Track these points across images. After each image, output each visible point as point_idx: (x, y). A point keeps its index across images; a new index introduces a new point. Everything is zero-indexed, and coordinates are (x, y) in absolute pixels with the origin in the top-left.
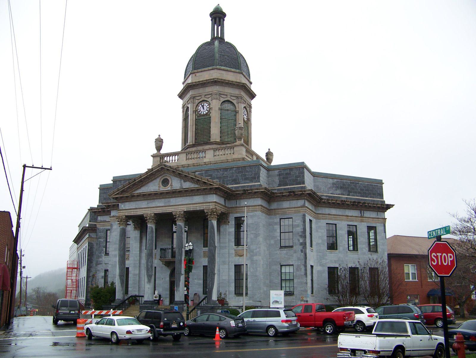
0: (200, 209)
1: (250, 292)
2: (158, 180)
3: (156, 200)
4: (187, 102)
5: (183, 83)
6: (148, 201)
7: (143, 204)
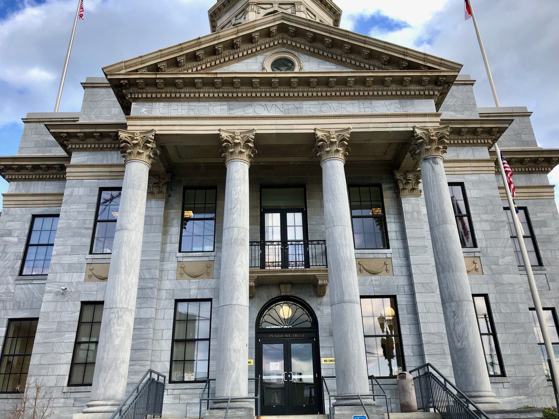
0: (395, 129)
1: (512, 369)
2: (260, 58)
4: (236, 17)
6: (230, 103)
7: (218, 109)
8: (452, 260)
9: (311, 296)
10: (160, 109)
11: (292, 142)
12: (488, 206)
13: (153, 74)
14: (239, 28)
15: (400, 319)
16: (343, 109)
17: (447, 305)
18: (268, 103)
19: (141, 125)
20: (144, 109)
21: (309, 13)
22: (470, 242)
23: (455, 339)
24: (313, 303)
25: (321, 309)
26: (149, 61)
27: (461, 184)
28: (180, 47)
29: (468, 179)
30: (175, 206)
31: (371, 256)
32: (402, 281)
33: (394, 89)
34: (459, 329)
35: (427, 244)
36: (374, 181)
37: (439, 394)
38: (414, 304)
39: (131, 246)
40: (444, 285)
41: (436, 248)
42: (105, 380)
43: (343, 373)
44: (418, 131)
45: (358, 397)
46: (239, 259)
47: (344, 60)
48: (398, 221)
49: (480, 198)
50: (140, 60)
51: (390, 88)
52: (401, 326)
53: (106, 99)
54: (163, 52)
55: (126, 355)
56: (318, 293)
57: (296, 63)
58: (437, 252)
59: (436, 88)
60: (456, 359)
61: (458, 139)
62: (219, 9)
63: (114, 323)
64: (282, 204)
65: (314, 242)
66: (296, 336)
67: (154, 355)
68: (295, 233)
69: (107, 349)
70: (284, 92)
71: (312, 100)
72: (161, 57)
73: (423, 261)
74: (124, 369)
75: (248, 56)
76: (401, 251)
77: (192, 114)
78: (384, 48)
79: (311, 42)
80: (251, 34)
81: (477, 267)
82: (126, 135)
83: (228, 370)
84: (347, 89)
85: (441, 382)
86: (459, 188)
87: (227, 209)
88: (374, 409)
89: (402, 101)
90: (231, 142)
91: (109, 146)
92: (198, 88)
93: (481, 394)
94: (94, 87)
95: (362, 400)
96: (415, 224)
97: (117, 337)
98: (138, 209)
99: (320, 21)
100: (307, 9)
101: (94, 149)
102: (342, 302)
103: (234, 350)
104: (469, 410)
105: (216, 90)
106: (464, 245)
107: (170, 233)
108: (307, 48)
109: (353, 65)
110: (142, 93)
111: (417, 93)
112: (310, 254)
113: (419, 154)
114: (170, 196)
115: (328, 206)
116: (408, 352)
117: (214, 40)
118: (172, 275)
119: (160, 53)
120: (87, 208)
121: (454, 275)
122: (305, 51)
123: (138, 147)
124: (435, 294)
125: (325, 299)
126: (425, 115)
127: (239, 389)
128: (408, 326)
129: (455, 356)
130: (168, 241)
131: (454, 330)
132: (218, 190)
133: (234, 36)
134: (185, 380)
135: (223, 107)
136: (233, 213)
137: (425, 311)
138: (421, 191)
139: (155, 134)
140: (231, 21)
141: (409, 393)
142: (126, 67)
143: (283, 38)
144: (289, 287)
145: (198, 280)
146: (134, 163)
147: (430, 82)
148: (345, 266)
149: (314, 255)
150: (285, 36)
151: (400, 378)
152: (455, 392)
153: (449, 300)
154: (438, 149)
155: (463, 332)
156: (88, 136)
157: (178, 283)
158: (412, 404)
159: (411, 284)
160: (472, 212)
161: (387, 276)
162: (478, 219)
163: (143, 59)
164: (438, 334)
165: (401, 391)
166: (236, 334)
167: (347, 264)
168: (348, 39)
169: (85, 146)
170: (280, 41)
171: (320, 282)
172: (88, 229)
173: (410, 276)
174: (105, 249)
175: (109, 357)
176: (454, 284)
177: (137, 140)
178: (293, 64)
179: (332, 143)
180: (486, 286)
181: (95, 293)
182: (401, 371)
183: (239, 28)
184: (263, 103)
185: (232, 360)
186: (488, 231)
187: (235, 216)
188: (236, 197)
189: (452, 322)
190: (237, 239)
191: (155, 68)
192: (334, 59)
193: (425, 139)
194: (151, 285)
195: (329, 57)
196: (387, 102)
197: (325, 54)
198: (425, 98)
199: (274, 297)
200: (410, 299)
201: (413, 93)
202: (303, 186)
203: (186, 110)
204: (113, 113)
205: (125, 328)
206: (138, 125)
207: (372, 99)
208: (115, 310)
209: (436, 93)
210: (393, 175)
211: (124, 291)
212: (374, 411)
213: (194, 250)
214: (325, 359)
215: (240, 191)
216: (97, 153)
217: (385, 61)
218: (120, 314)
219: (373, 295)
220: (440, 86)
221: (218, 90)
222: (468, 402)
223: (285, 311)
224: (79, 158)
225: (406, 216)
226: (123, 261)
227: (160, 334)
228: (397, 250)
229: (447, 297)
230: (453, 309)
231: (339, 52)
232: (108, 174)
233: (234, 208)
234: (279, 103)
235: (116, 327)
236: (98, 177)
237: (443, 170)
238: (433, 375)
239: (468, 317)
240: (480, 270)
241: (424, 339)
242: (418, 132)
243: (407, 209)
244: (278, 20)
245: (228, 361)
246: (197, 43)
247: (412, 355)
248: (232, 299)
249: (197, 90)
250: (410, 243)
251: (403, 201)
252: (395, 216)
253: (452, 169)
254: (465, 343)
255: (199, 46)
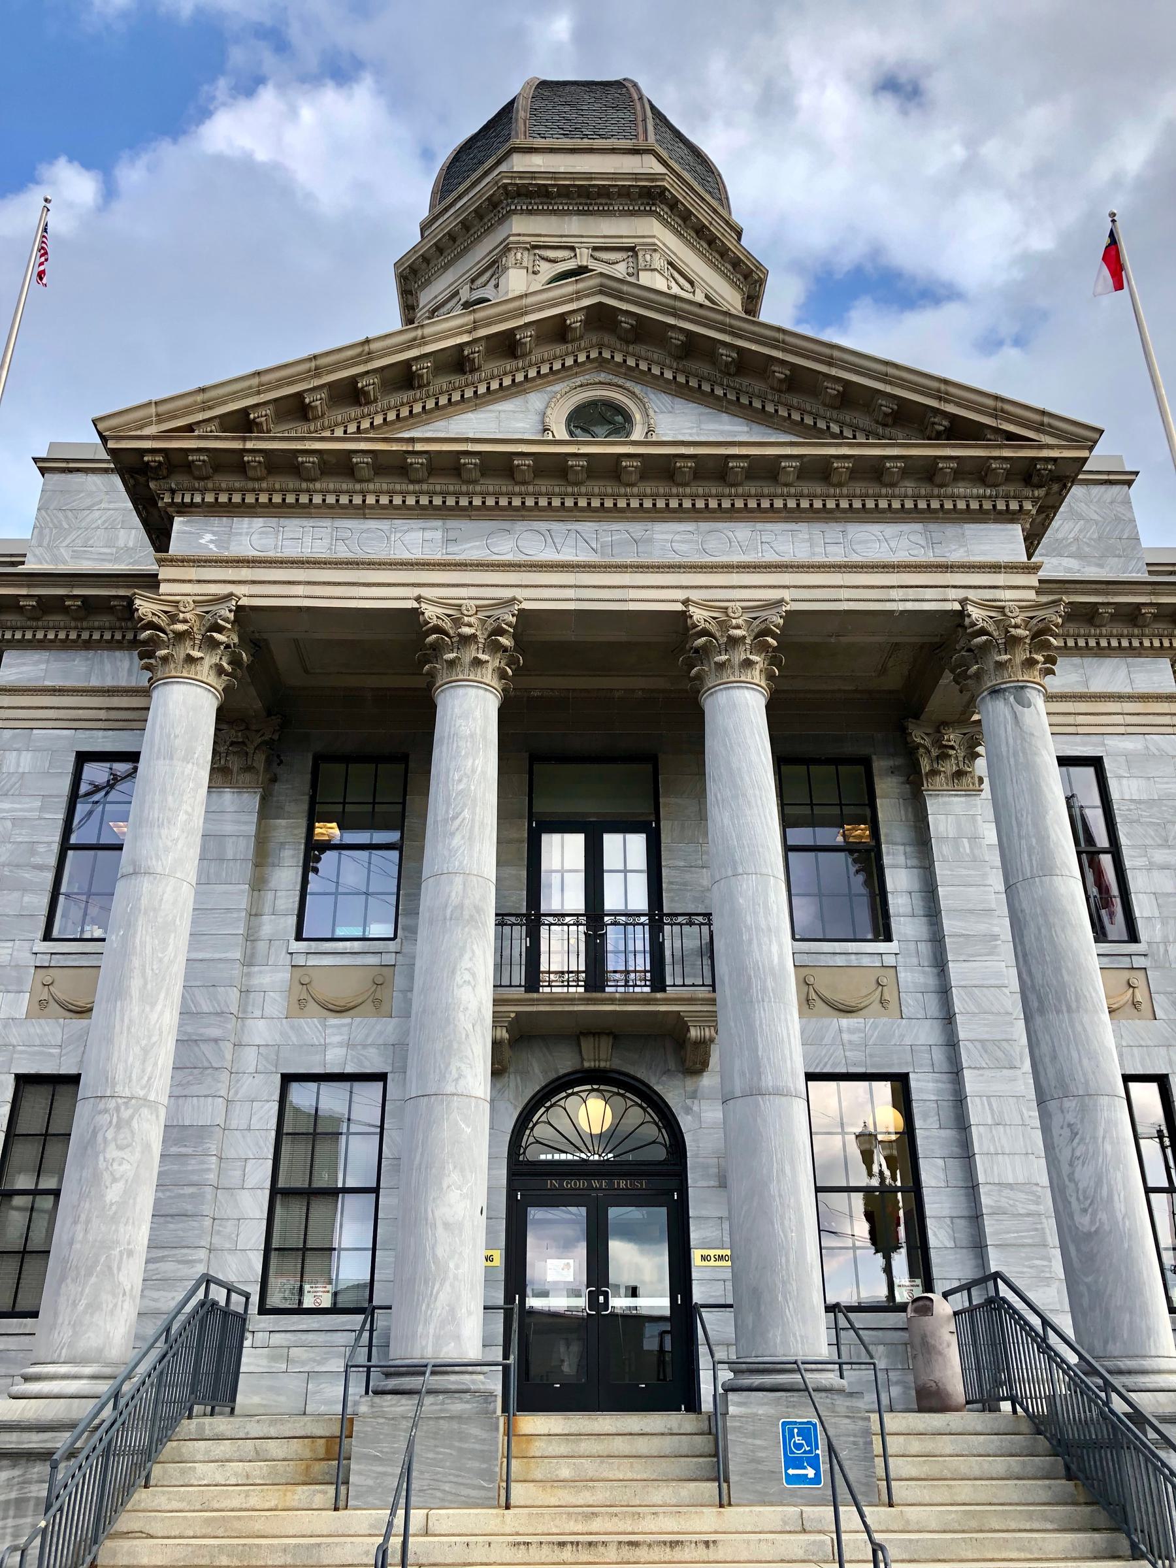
0: (910, 606)
2: (535, 400)
3: (520, 526)
4: (473, 281)
5: (424, 228)
6: (451, 524)
7: (416, 539)
8: (1066, 977)
9: (667, 1072)
10: (252, 536)
11: (622, 636)
12: (1169, 826)
13: (233, 439)
14: (480, 315)
15: (919, 1141)
16: (766, 546)
17: (1052, 1105)
18: (555, 526)
19: (199, 581)
20: (209, 536)
21: (676, 275)
22: (1117, 927)
23: (1075, 1205)
24: (673, 1093)
25: (695, 1108)
26: (225, 403)
27: (1097, 763)
28: (313, 364)
29: (1115, 750)
30: (290, 807)
31: (840, 961)
32: (927, 1033)
33: (910, 492)
34: (1085, 1175)
35: (996, 930)
36: (849, 749)
37: (1026, 1361)
38: (959, 1101)
39: (160, 920)
40: (1045, 1048)
41: (1022, 943)
42: (75, 1304)
43: (751, 1298)
44: (975, 613)
45: (795, 1367)
46: (465, 963)
47: (770, 408)
48: (915, 862)
49: (1151, 803)
50: (199, 398)
51: (897, 491)
52: (921, 1161)
53: (103, 506)
54: (265, 378)
55: (138, 1232)
56: (688, 1064)
57: (638, 416)
58: (1025, 955)
59: (1028, 492)
60: (1075, 1260)
61: (1087, 637)
62: (425, 259)
63: (105, 1139)
64: (590, 807)
65: (680, 919)
66: (622, 1185)
67: (219, 1232)
68: (626, 892)
69: (83, 1217)
70: (602, 496)
71: (680, 520)
72: (259, 393)
73: (987, 976)
74: (132, 1273)
75: (505, 393)
76: (925, 948)
77: (343, 553)
78: (884, 378)
79: (678, 358)
80: (511, 332)
81: (1139, 998)
82: (156, 607)
83: (426, 1282)
84: (779, 491)
85: (1032, 1329)
86: (1090, 771)
87: (436, 822)
88: (842, 1403)
89: (932, 526)
90: (451, 632)
91: (107, 636)
92: (360, 481)
93: (1147, 1364)
94: (70, 471)
95: (808, 1376)
96: (964, 872)
97: (115, 1180)
98: (182, 817)
99: (707, 297)
100: (670, 264)
101: (66, 645)
102: (755, 1092)
103: (447, 1225)
104: (1112, 1411)
105: (411, 487)
106: (1100, 934)
107: (272, 885)
108: (668, 375)
109: (795, 423)
110: (203, 491)
111: (974, 505)
112: (668, 953)
113: (978, 676)
114: (274, 780)
115: (719, 816)
116: (938, 1236)
117: (409, 348)
118: (276, 1003)
119: (255, 381)
120: (42, 809)
121: (1071, 1020)
122: (661, 382)
123: (188, 643)
124: (1019, 1072)
125: (708, 1081)
126: (995, 568)
127: (457, 1338)
128: (940, 1162)
129: (1072, 1249)
130: (267, 909)
131: (1071, 1177)
132: (412, 765)
133: (466, 338)
134: (305, 1306)
135: (428, 535)
136: (453, 834)
137: (990, 1122)
138: (981, 780)
139: (238, 607)
140: (457, 293)
141: (940, 1353)
142: (160, 418)
143: (601, 346)
144: (606, 1043)
145: (348, 1020)
146: (176, 687)
147: (1009, 477)
148: (764, 990)
149: (678, 953)
150: (607, 338)
151: (916, 1310)
152: (1073, 1359)
153: (1056, 1094)
154: (1030, 663)
155: (1099, 1183)
156: (48, 606)
157: (292, 1027)
158: (950, 1388)
159: (952, 1044)
160: (1123, 840)
161: (884, 1020)
162: (1141, 862)
163: (207, 395)
164: (1026, 1186)
165: (916, 1349)
166: (453, 1177)
167: (770, 983)
168: (784, 350)
169: (40, 635)
170: (594, 355)
171: (694, 1033)
172: (40, 868)
173: (948, 1018)
174: (87, 928)
175: (90, 1238)
176: (1072, 1046)
177: (185, 621)
178: (628, 418)
179: (734, 642)
180: (1163, 1051)
181: (56, 1051)
182: (918, 1292)
183: (480, 315)
184: (542, 526)
185: (440, 1252)
186: (1169, 895)
187: (456, 841)
188: (461, 787)
189: (1065, 1155)
190: (461, 906)
191: (242, 422)
192: (742, 406)
193: (995, 634)
194: (215, 1032)
195: (730, 402)
196: (890, 530)
197: (719, 392)
198: (996, 521)
199: (562, 1072)
200: (949, 1086)
201: (961, 505)
202: (651, 759)
203: (326, 541)
204: (121, 543)
205: (138, 1155)
206: (190, 581)
207: (848, 520)
208: (112, 1104)
209: (1028, 506)
210: (904, 732)
211: (137, 1049)
212: (842, 1410)
213: (340, 932)
214: (706, 1252)
215: (473, 771)
216: (71, 654)
217: (886, 415)
218: (126, 1114)
219: (844, 1070)
220: (1040, 486)
221: (417, 487)
222: (1108, 1387)
223: (593, 1113)
224: (24, 669)
225: (939, 850)
226: (136, 962)
227: (238, 1173)
228: (912, 946)
229: (1053, 1084)
230: (1070, 1118)
231: (758, 386)
232: (102, 714)
233: (454, 818)
234: (587, 528)
235: (112, 1152)
236: (76, 724)
237: (1045, 720)
238: (1010, 1306)
239: (1112, 1143)
240: (1146, 1006)
241: (985, 1200)
242: (974, 616)
243: (942, 828)
244: (587, 296)
245: (429, 1256)
246: (360, 355)
247: (952, 1245)
248: (443, 1078)
249: (358, 487)
250: (949, 925)
251: (932, 805)
252: (908, 849)
253: (1070, 720)
254: (1102, 1216)
255: (366, 362)
